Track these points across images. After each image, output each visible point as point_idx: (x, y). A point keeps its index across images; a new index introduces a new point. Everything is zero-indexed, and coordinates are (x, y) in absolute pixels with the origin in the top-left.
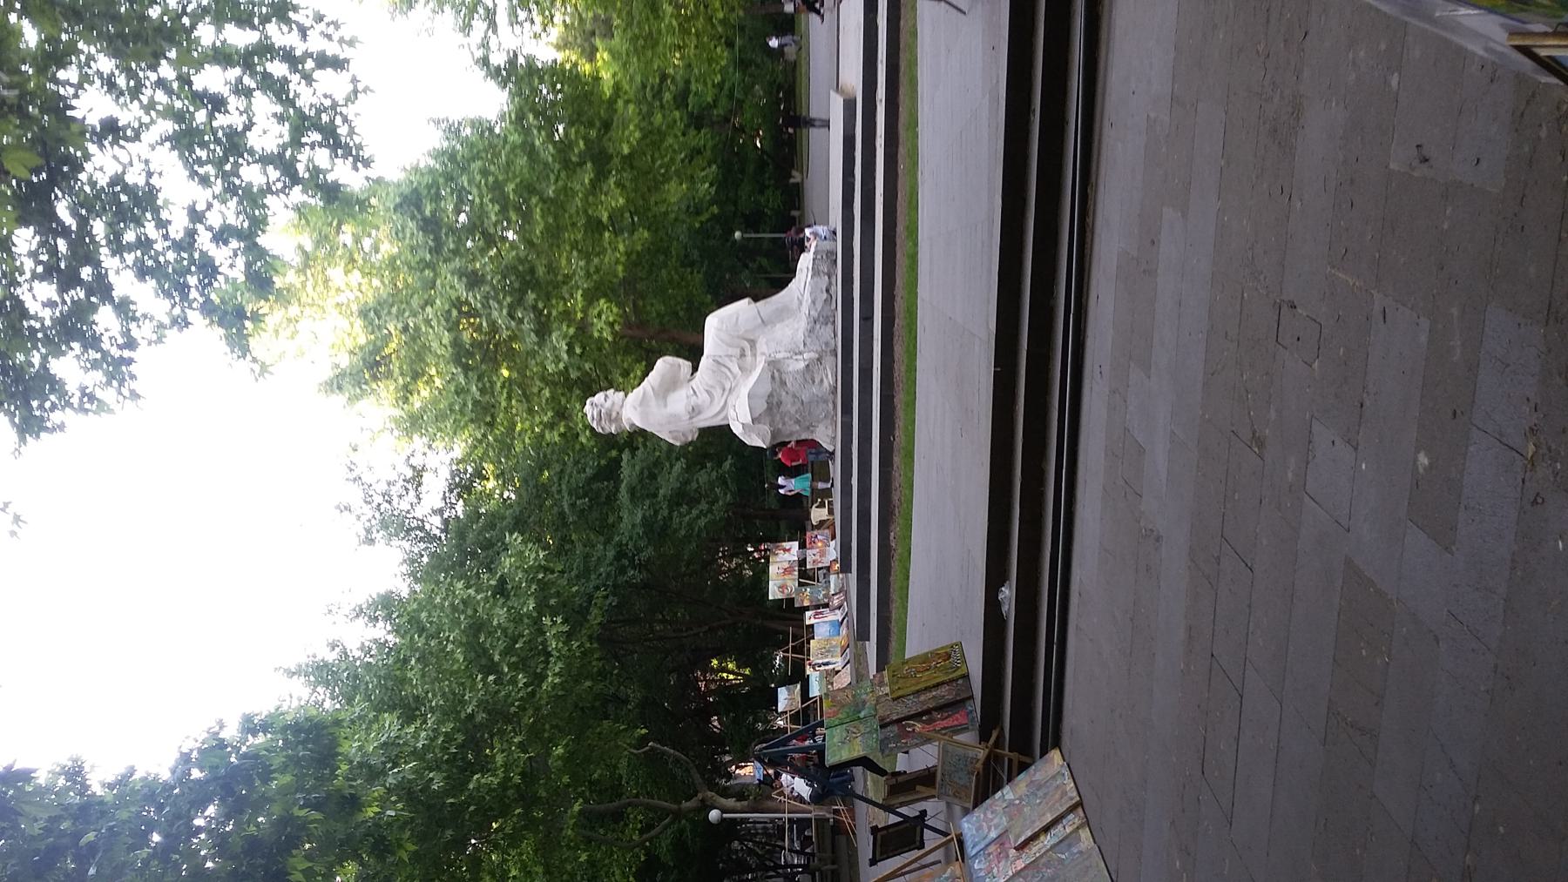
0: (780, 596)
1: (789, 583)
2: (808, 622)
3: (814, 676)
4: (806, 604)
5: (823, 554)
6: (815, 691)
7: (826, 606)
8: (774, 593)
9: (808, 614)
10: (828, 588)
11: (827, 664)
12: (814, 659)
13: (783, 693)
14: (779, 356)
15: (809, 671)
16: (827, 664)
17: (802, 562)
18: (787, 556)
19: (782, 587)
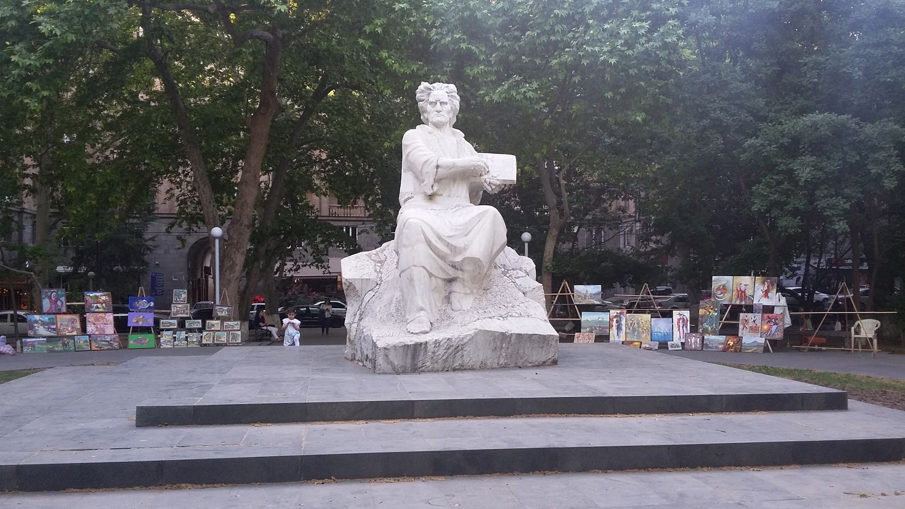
0: (714, 286)
1: (727, 296)
2: (675, 313)
3: (604, 317)
4: (701, 312)
5: (754, 330)
6: (586, 317)
7: (694, 330)
8: (718, 281)
9: (687, 314)
10: (714, 333)
11: (619, 328)
12: (626, 318)
13: (596, 289)
14: (366, 299)
15: (613, 312)
16: (619, 328)
17: (750, 309)
18: (759, 293)
19: (724, 289)
